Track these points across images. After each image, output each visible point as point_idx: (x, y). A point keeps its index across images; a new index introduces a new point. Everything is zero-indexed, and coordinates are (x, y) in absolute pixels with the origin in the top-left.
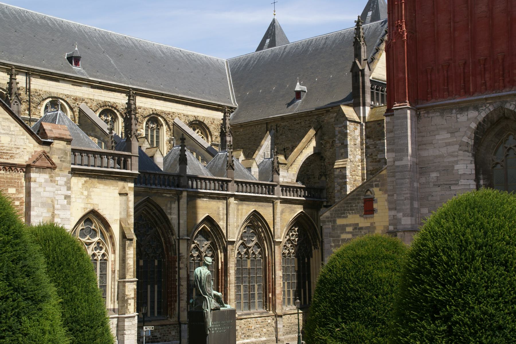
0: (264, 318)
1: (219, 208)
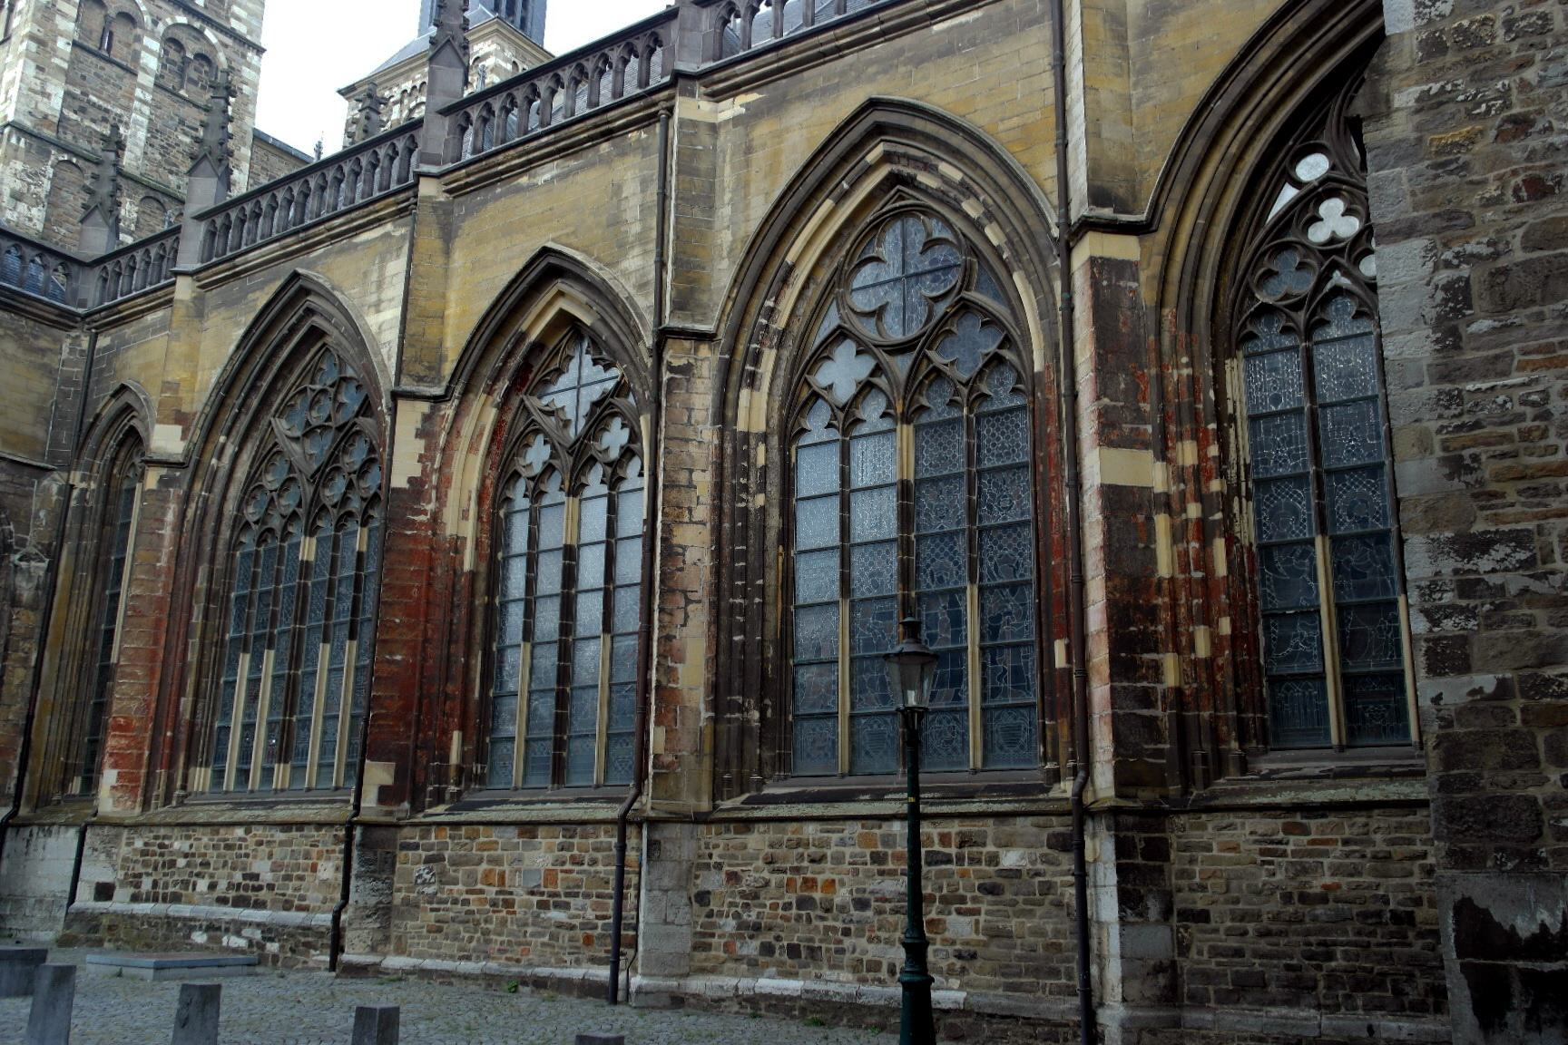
0: (954, 828)
1: (617, 189)
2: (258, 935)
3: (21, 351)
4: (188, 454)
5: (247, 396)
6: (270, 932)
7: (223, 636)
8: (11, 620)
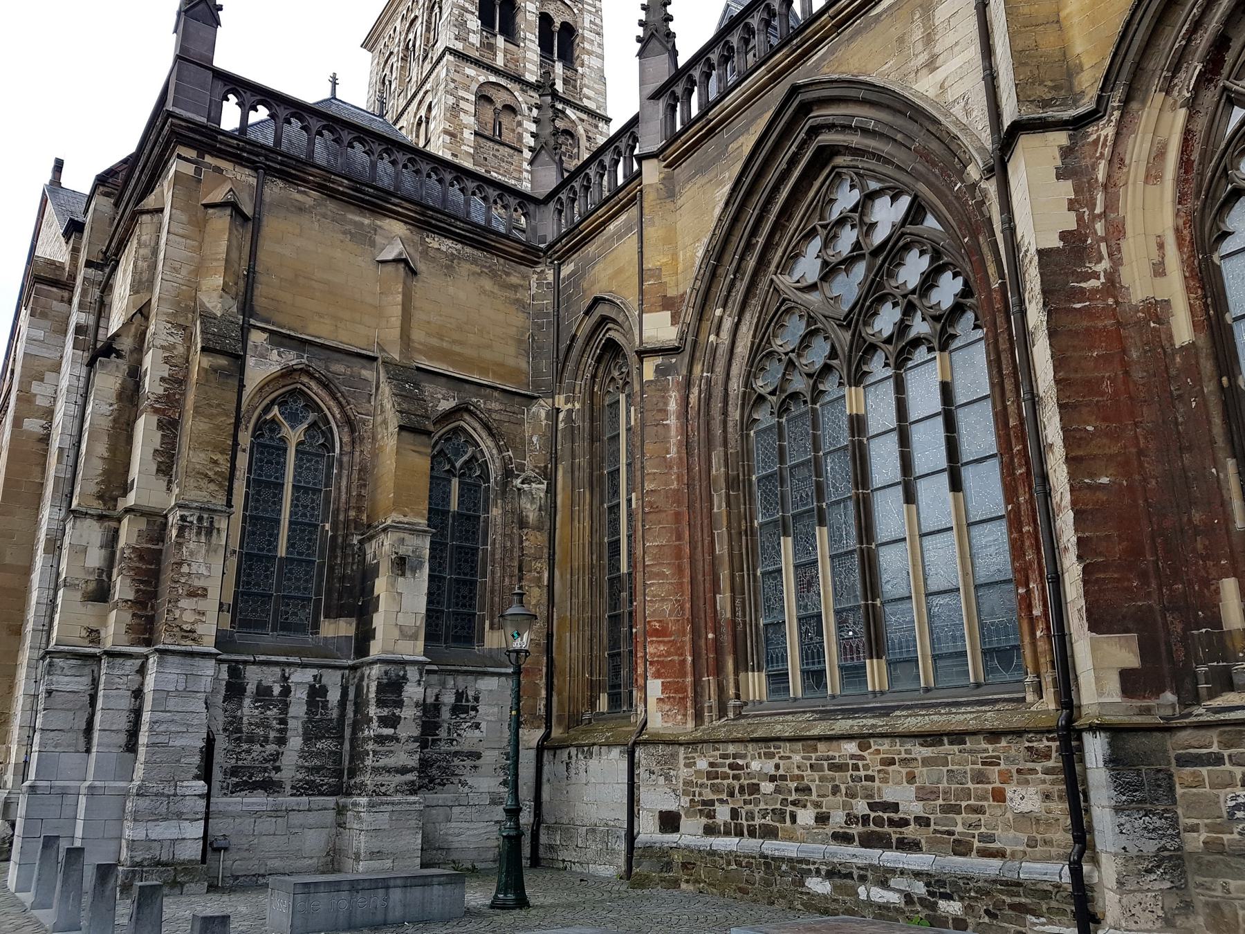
2: (920, 889)
3: (496, 287)
4: (682, 337)
5: (742, 258)
6: (939, 886)
7: (752, 522)
8: (521, 542)
